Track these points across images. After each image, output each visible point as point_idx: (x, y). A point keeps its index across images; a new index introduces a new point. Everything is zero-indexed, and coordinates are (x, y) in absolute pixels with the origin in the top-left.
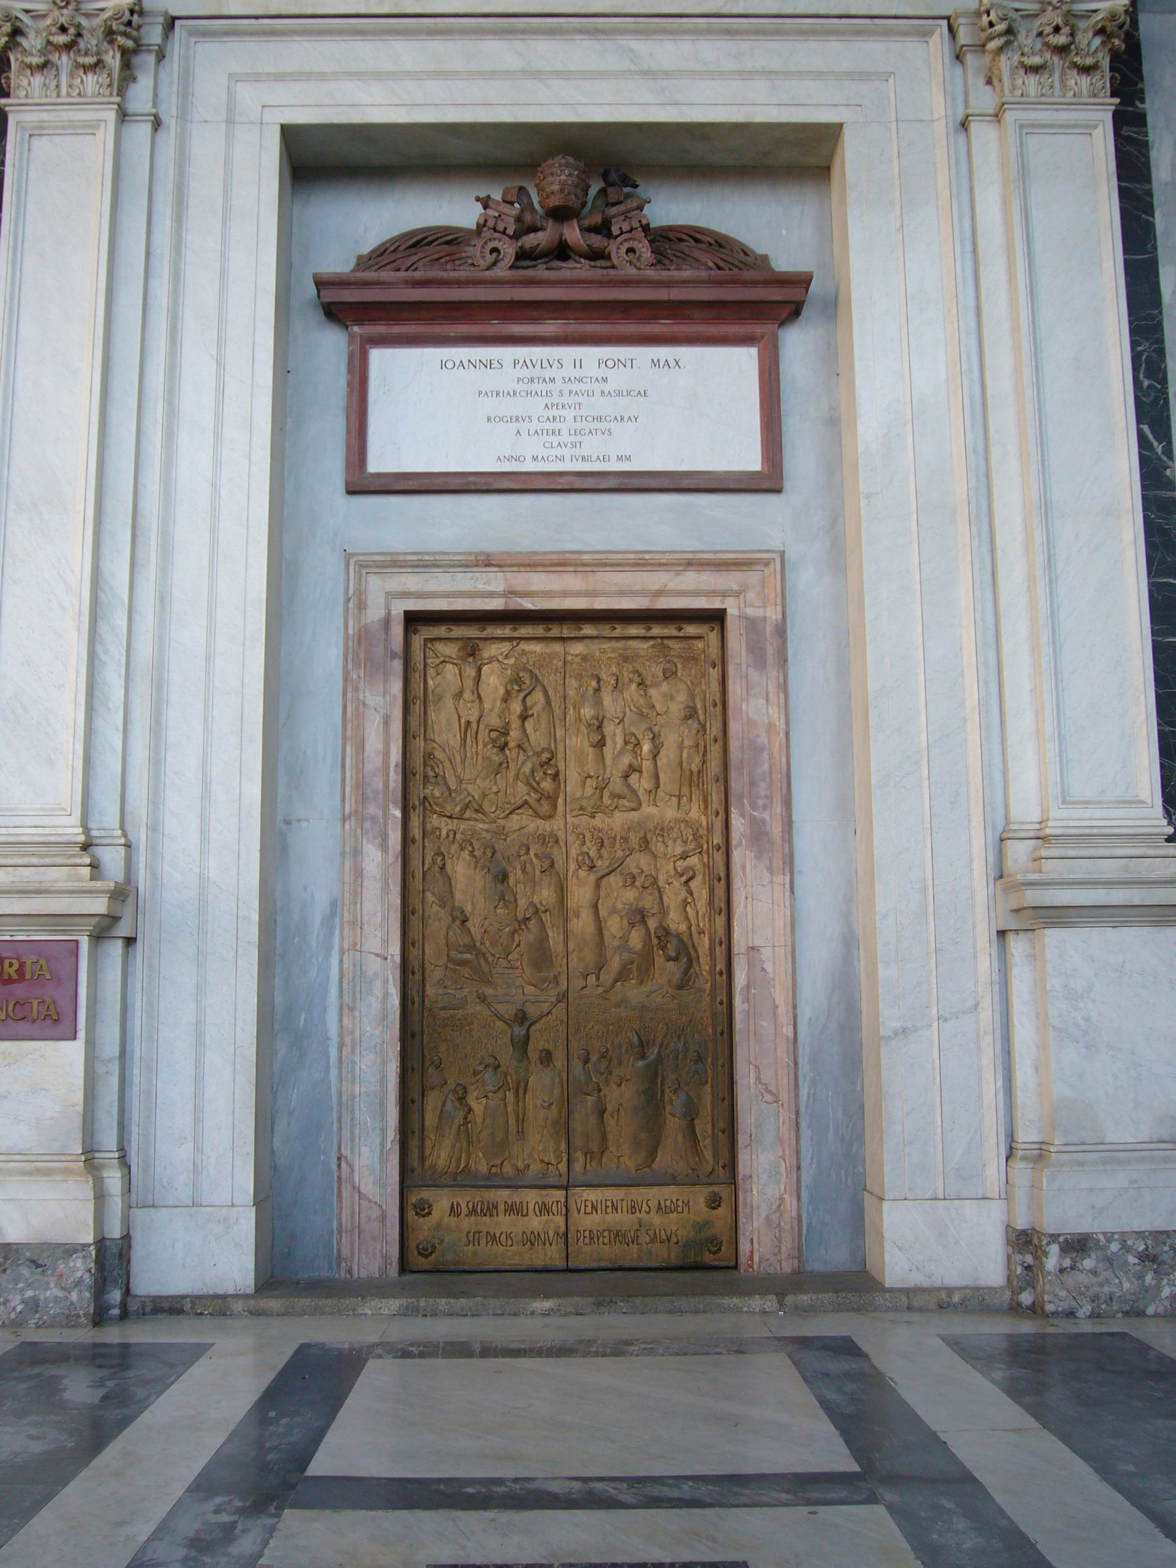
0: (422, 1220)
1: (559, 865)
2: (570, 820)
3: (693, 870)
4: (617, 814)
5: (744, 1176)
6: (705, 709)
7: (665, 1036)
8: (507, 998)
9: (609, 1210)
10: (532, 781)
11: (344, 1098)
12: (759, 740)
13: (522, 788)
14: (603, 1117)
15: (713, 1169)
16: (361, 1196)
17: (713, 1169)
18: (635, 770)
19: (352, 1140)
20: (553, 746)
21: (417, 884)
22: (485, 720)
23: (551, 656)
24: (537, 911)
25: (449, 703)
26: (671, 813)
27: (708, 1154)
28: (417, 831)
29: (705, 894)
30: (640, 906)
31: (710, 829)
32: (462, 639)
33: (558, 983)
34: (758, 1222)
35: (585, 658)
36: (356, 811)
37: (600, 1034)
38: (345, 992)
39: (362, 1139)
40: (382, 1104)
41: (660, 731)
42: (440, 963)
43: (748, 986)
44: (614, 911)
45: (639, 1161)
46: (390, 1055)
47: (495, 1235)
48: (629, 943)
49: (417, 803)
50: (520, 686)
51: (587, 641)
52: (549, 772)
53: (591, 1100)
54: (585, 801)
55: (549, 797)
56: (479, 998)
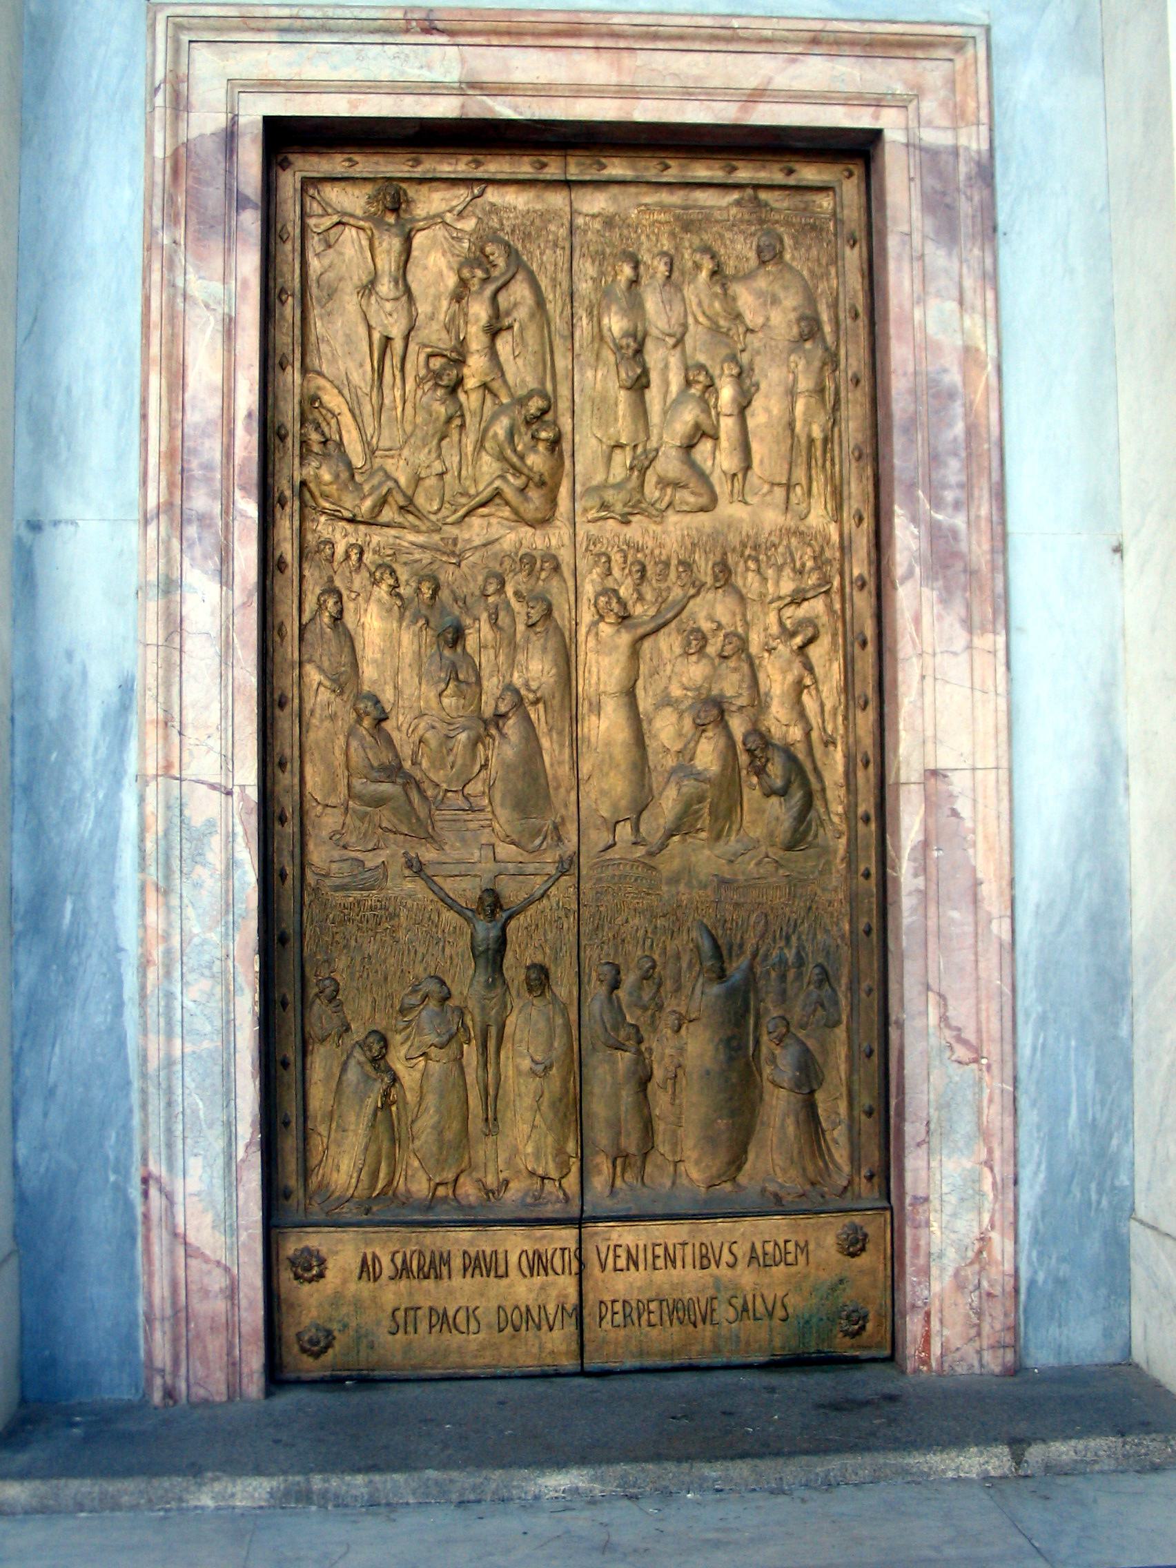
0: (306, 1288)
1: (562, 614)
3: (815, 627)
4: (672, 518)
5: (915, 1198)
7: (762, 937)
8: (462, 868)
9: (660, 1263)
10: (509, 453)
11: (153, 1065)
13: (488, 465)
15: (850, 1182)
16: (190, 1252)
18: (704, 435)
19: (170, 1145)
20: (549, 386)
21: (290, 649)
22: (423, 334)
23: (546, 217)
24: (519, 703)
25: (350, 302)
26: (772, 518)
27: (841, 1155)
29: (836, 668)
30: (715, 692)
31: (845, 548)
33: (560, 839)
34: (940, 1283)
36: (170, 504)
37: (641, 933)
38: (151, 861)
39: (189, 1141)
40: (227, 1075)
42: (332, 801)
43: (926, 845)
44: (666, 701)
45: (714, 1169)
46: (240, 979)
47: (445, 1314)
49: (288, 493)
50: (487, 271)
51: (615, 190)
52: (543, 435)
53: (624, 1059)
54: (611, 492)
55: (542, 484)
56: (410, 867)
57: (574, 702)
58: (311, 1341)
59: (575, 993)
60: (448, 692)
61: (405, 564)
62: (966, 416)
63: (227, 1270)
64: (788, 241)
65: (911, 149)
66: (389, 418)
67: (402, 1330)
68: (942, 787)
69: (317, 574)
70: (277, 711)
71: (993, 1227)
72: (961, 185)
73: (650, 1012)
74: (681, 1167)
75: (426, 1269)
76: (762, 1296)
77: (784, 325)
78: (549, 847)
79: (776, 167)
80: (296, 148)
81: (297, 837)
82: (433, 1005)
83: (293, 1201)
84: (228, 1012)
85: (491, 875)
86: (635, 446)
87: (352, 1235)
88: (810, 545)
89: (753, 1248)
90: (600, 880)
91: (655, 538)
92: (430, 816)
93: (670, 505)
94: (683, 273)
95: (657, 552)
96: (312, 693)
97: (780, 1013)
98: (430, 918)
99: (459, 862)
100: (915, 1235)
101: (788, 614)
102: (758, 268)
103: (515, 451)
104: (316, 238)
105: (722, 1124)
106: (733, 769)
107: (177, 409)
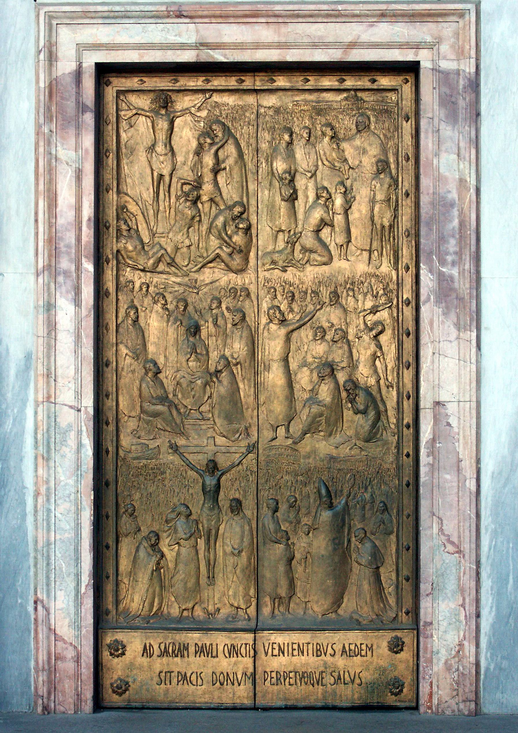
0: (116, 660)
1: (250, 319)
2: (261, 274)
4: (309, 268)
5: (425, 622)
6: (398, 163)
7: (353, 486)
8: (198, 449)
9: (296, 653)
12: (450, 196)
13: (214, 242)
14: (291, 564)
15: (397, 615)
16: (57, 638)
17: (397, 615)
18: (326, 224)
19: (48, 585)
21: (112, 337)
22: (180, 173)
23: (244, 108)
24: (228, 364)
25: (142, 156)
27: (392, 601)
28: (111, 284)
29: (393, 347)
30: (330, 359)
31: (399, 284)
32: (154, 91)
33: (248, 434)
34: (438, 666)
35: (277, 111)
36: (50, 266)
37: (289, 484)
39: (57, 583)
40: (77, 551)
41: (352, 186)
42: (133, 414)
43: (434, 440)
44: (304, 364)
45: (325, 606)
46: (84, 503)
48: (319, 396)
49: (110, 256)
50: (212, 139)
51: (280, 93)
52: (241, 226)
54: (277, 255)
55: (241, 251)
56: (172, 448)
57: (256, 365)
58: (117, 687)
59: (255, 514)
60: (192, 359)
61: (171, 293)
62: (459, 216)
63: (75, 647)
64: (372, 119)
65: (434, 72)
66: (163, 217)
67: (163, 683)
68: (442, 410)
69: (125, 298)
70: (105, 368)
71: (465, 639)
72: (461, 92)
73: (294, 524)
74: (309, 605)
75: (176, 652)
76: (348, 672)
77: (369, 165)
78: (243, 439)
79: (366, 79)
80: (114, 74)
81: (115, 432)
82: (183, 519)
83: (110, 617)
84: (78, 519)
85: (213, 453)
86: (290, 231)
87: (139, 634)
88: (381, 282)
89: (344, 647)
90: (269, 456)
91: (300, 280)
92: (182, 422)
93: (308, 261)
94: (316, 138)
95: (300, 286)
96: (123, 359)
97: (362, 526)
98: (181, 475)
99: (197, 446)
100: (425, 641)
101: (369, 319)
102: (356, 134)
103: (227, 234)
104: (124, 122)
105: (329, 582)
106: (338, 399)
107: (53, 217)
